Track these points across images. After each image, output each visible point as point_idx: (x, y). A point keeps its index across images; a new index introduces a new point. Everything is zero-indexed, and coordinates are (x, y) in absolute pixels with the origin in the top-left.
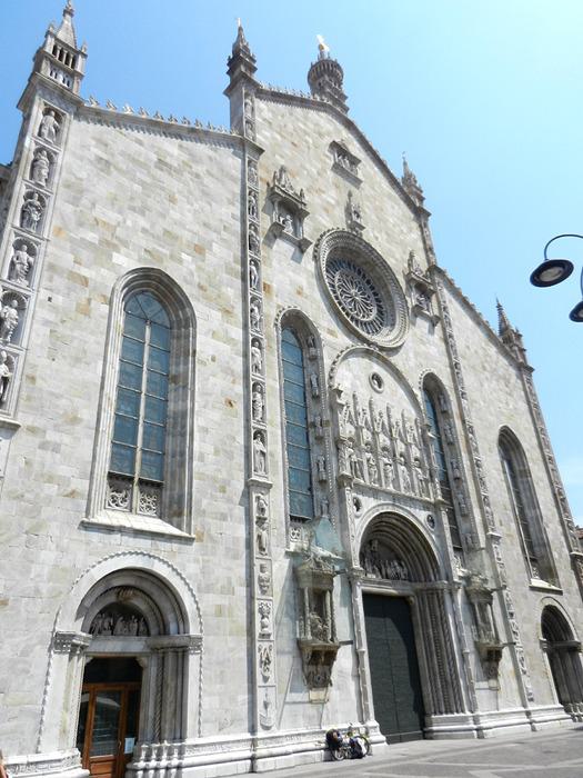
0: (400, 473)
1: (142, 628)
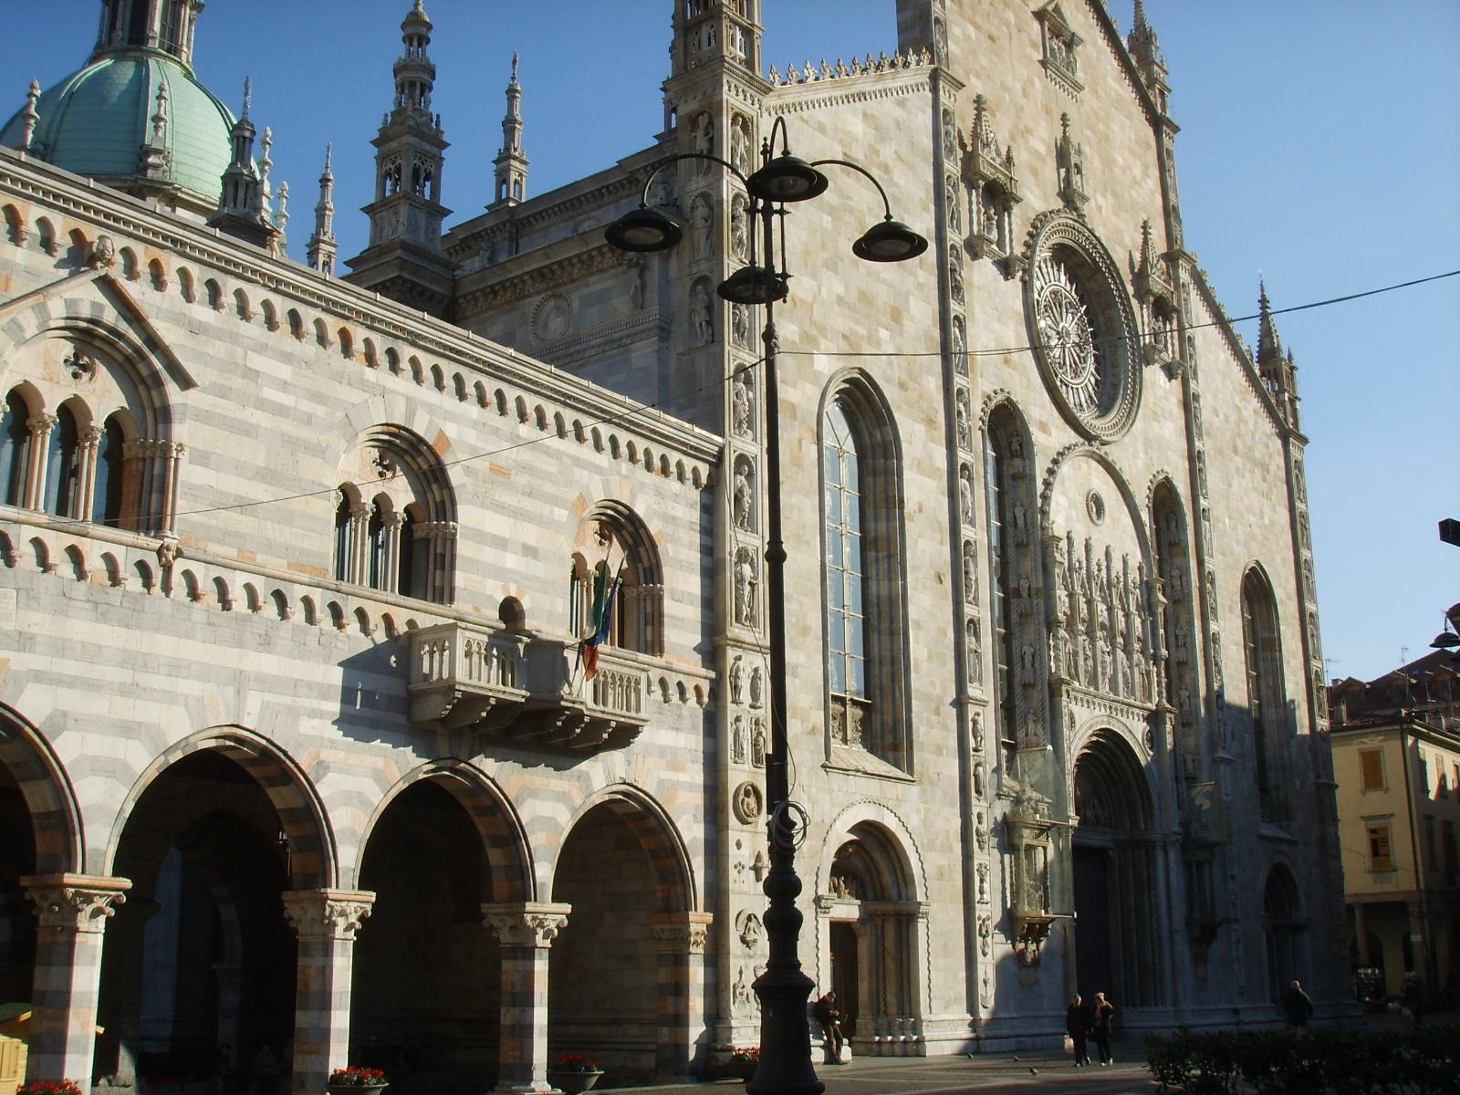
0: (1120, 667)
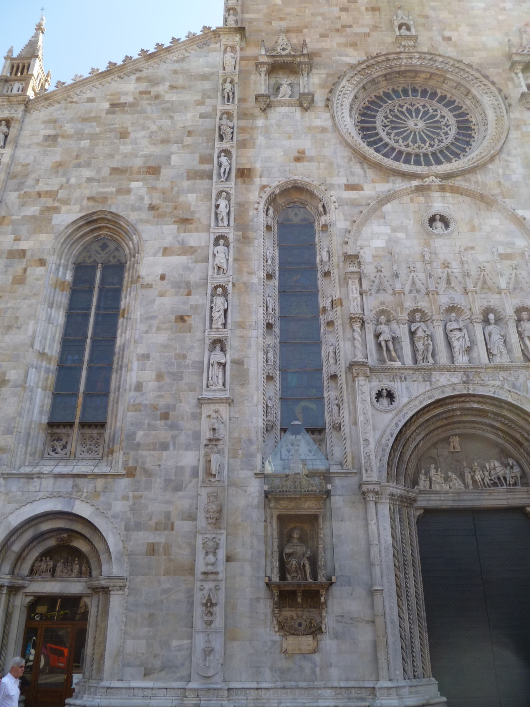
1: (84, 569)
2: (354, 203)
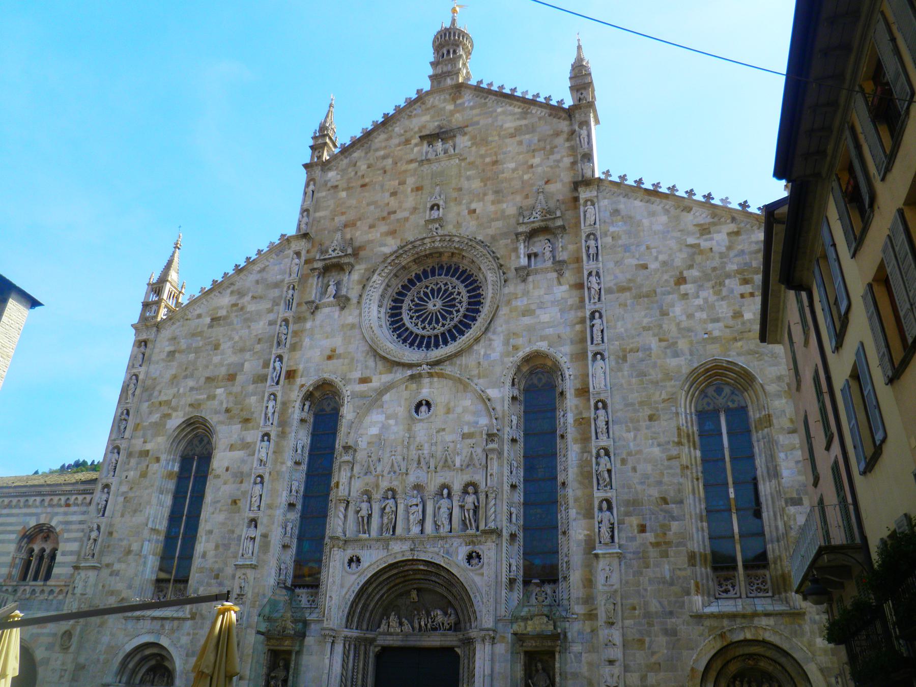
2: (362, 396)
